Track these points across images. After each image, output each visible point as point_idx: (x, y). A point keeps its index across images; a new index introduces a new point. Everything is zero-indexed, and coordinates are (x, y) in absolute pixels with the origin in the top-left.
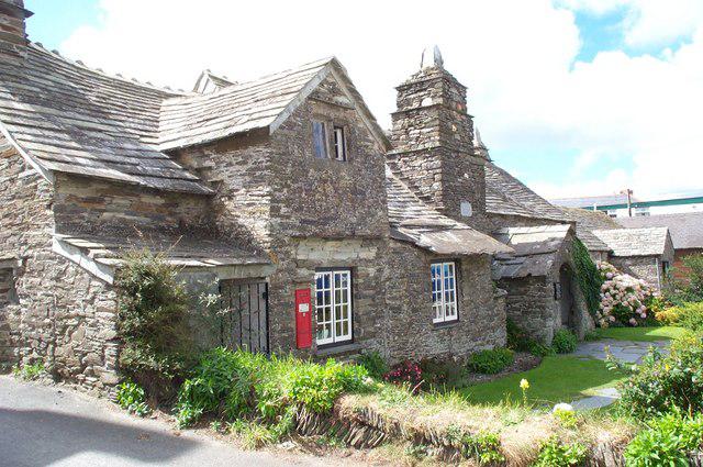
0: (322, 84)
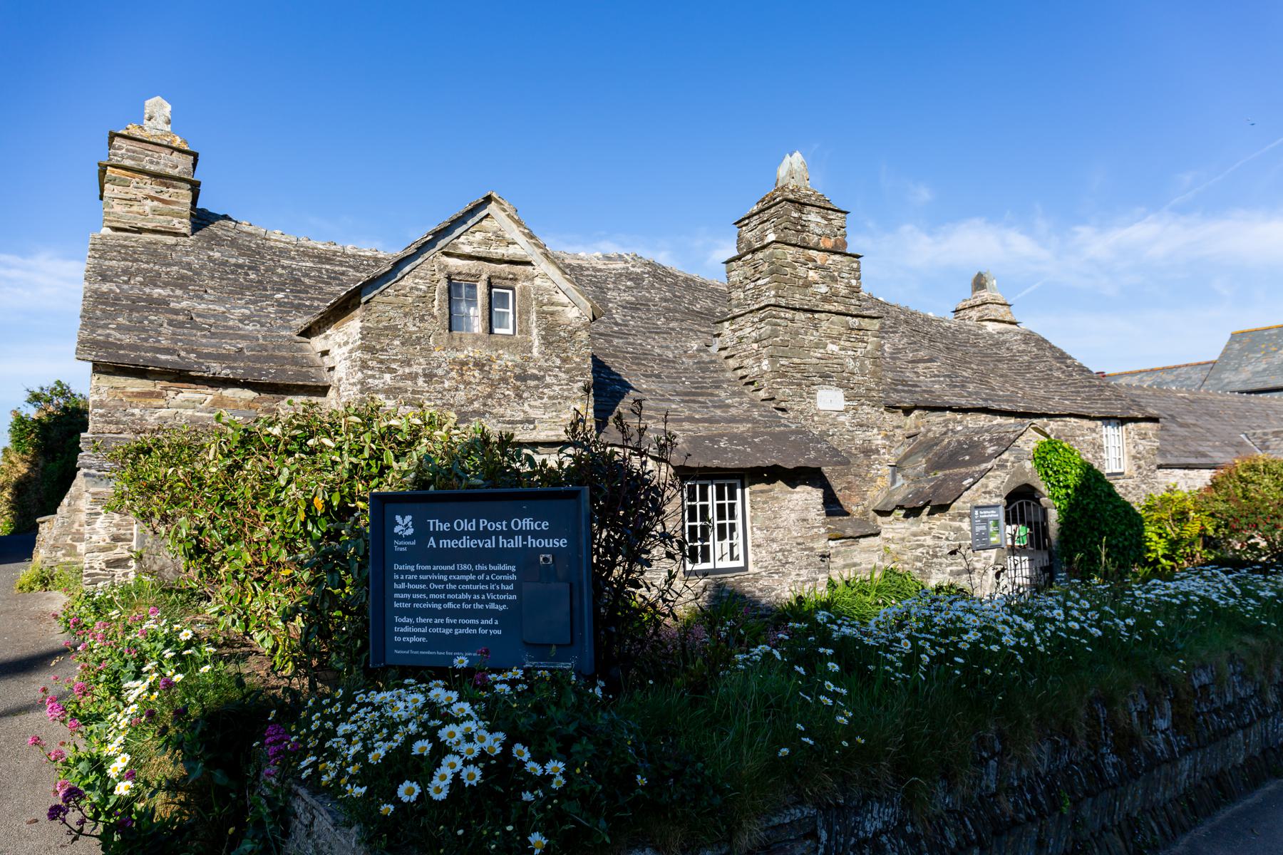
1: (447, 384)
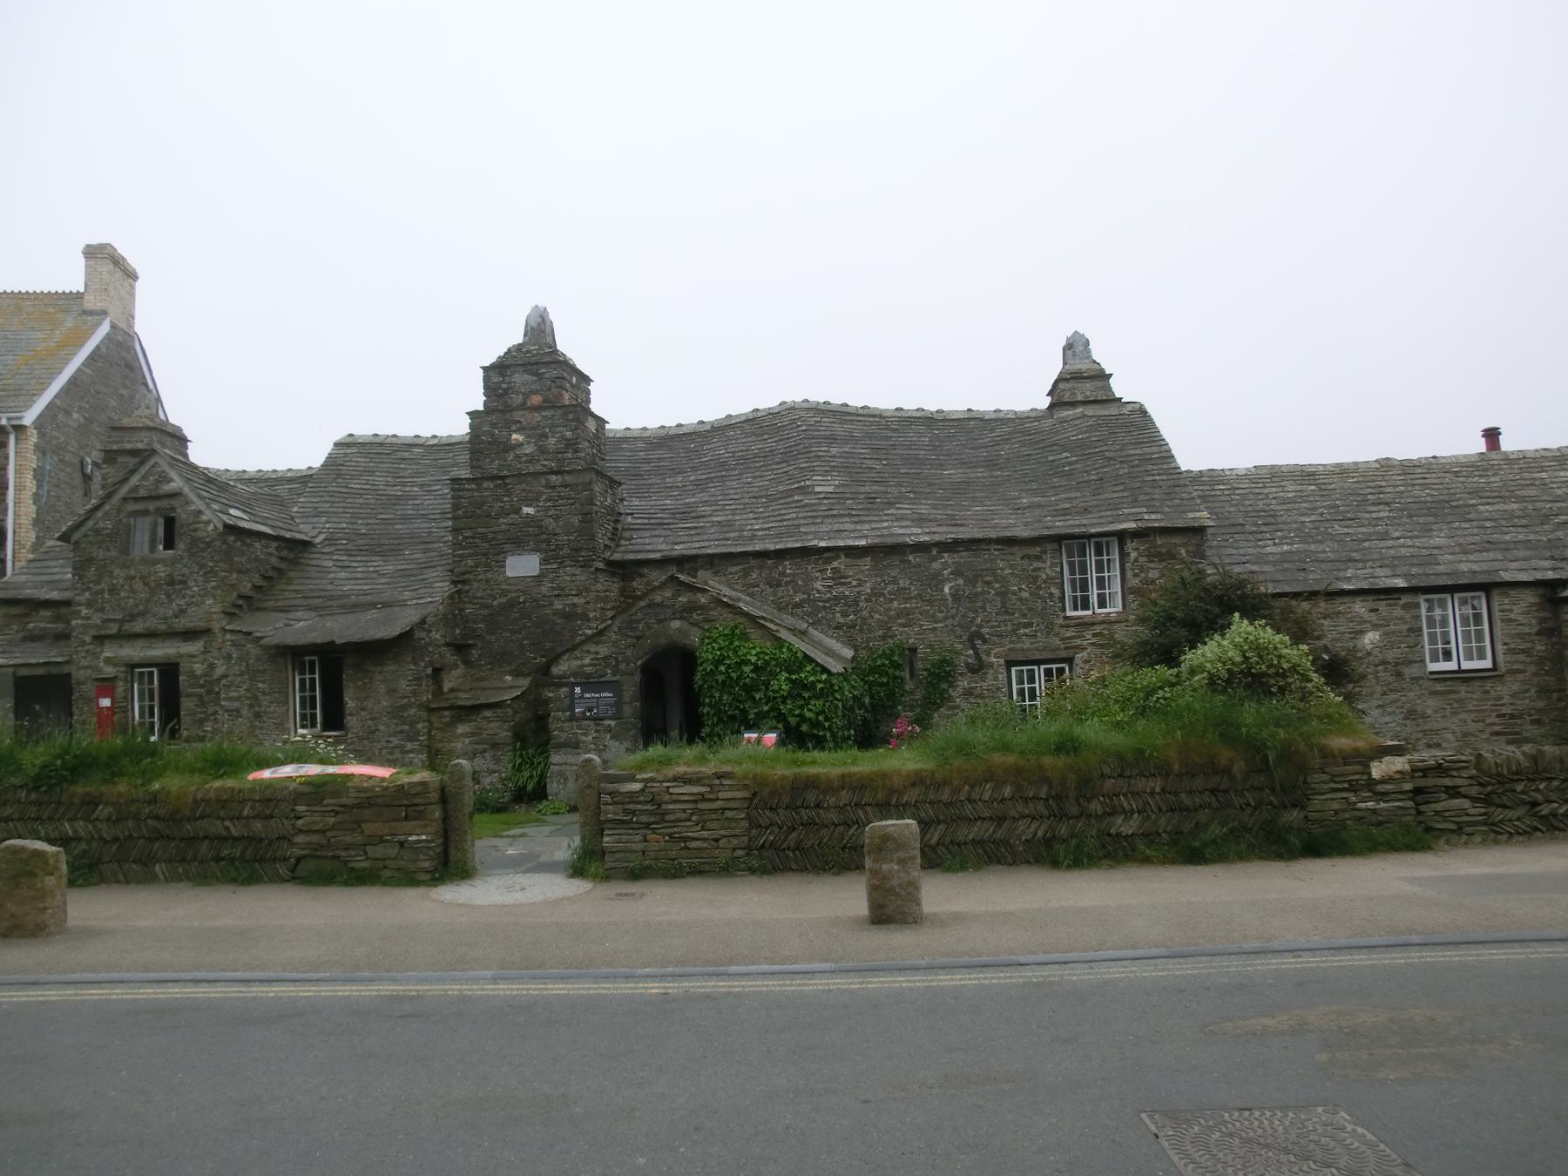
0: (144, 478)
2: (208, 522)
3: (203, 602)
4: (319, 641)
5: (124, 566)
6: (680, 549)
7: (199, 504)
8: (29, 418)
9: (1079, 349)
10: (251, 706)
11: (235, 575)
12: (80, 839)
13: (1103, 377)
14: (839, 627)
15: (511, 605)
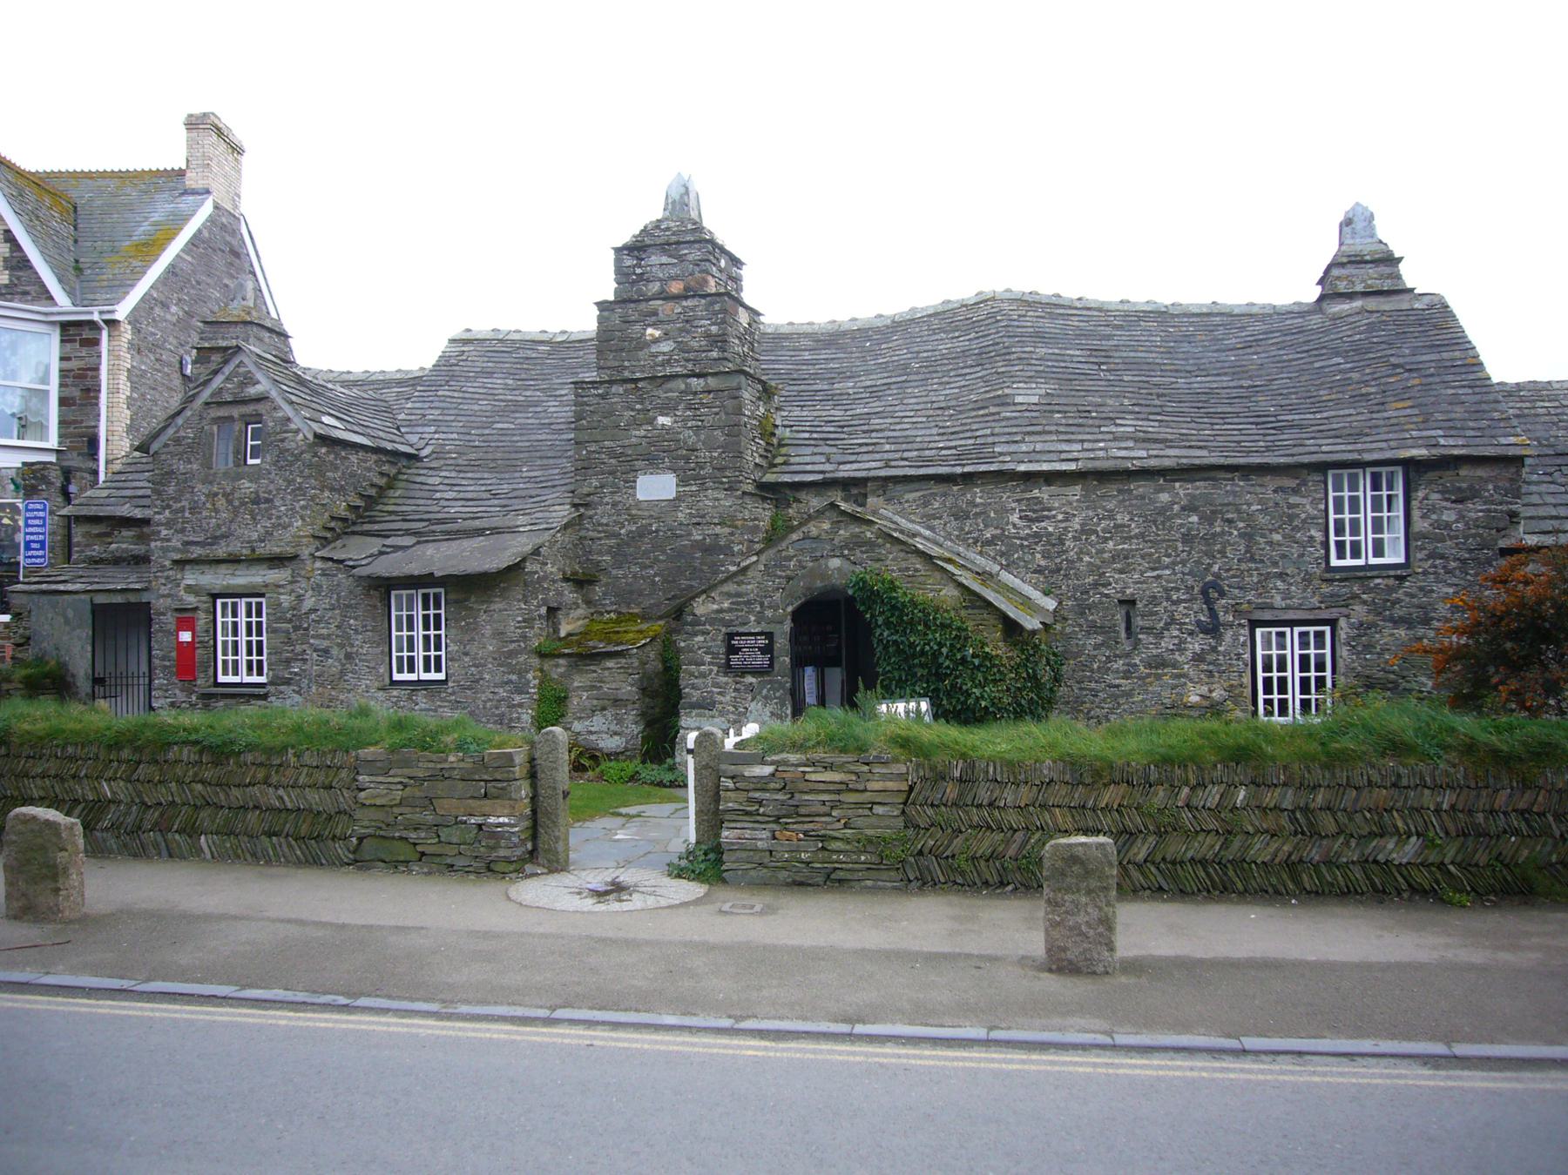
0: (228, 379)
1: (205, 513)
2: (297, 431)
3: (290, 525)
4: (416, 573)
5: (207, 481)
6: (846, 471)
7: (288, 411)
8: (122, 311)
9: (1359, 225)
10: (342, 646)
11: (327, 493)
12: (120, 802)
13: (1390, 261)
14: (1039, 571)
15: (642, 533)
